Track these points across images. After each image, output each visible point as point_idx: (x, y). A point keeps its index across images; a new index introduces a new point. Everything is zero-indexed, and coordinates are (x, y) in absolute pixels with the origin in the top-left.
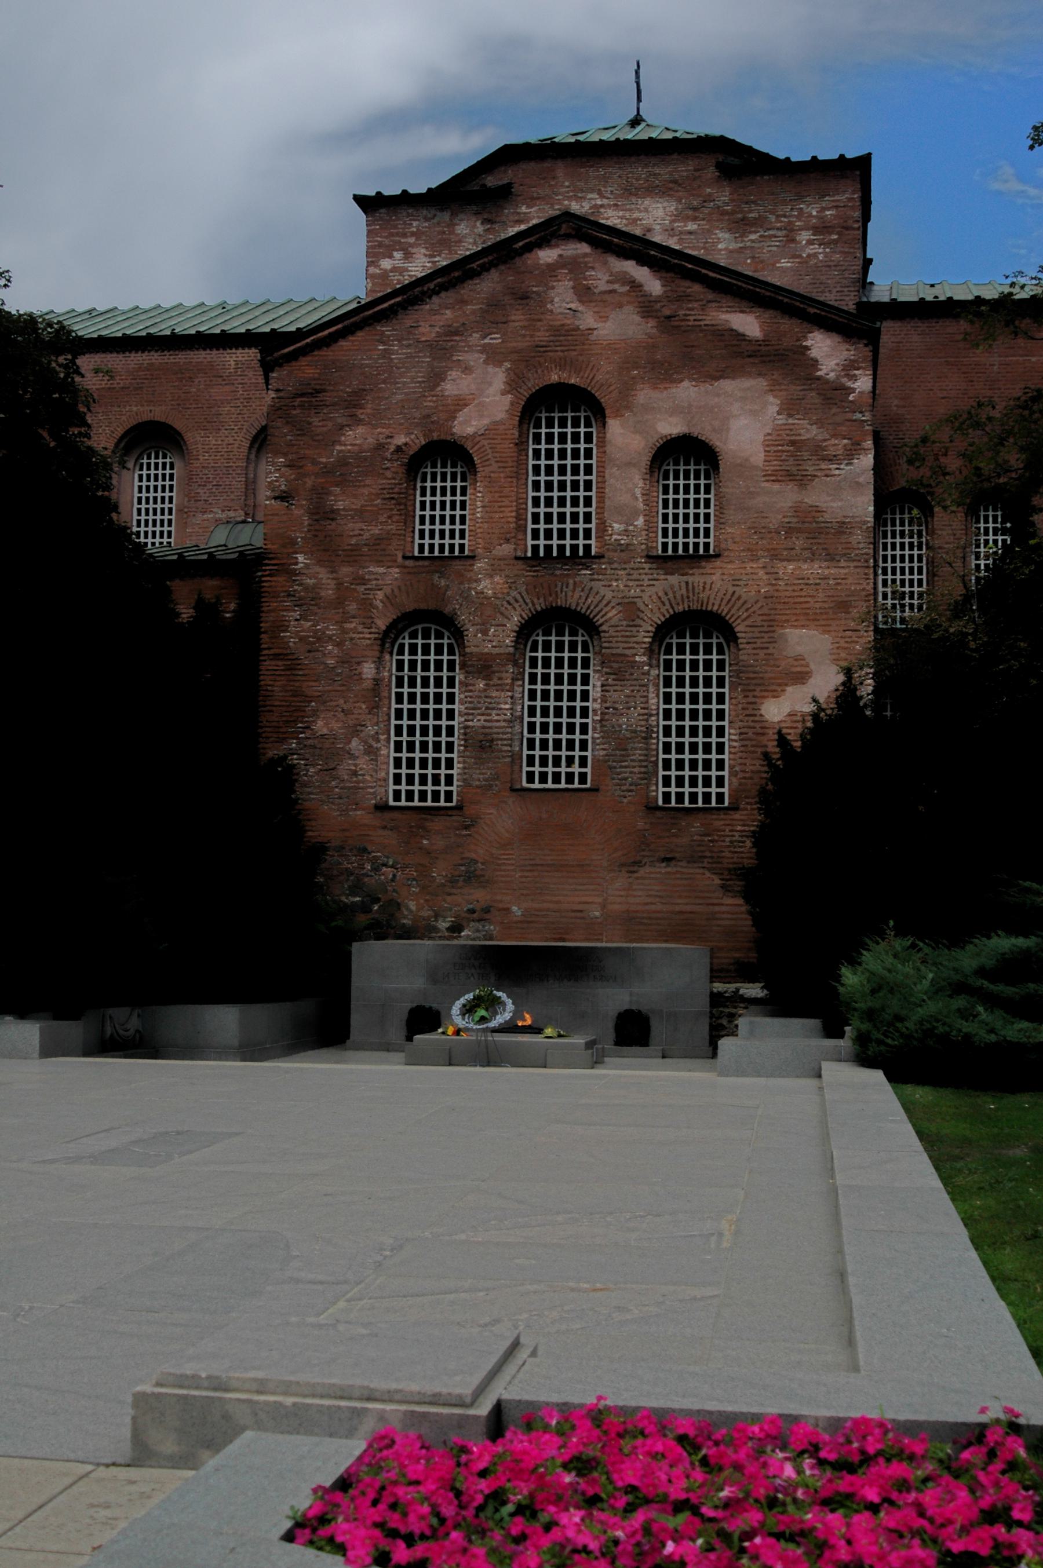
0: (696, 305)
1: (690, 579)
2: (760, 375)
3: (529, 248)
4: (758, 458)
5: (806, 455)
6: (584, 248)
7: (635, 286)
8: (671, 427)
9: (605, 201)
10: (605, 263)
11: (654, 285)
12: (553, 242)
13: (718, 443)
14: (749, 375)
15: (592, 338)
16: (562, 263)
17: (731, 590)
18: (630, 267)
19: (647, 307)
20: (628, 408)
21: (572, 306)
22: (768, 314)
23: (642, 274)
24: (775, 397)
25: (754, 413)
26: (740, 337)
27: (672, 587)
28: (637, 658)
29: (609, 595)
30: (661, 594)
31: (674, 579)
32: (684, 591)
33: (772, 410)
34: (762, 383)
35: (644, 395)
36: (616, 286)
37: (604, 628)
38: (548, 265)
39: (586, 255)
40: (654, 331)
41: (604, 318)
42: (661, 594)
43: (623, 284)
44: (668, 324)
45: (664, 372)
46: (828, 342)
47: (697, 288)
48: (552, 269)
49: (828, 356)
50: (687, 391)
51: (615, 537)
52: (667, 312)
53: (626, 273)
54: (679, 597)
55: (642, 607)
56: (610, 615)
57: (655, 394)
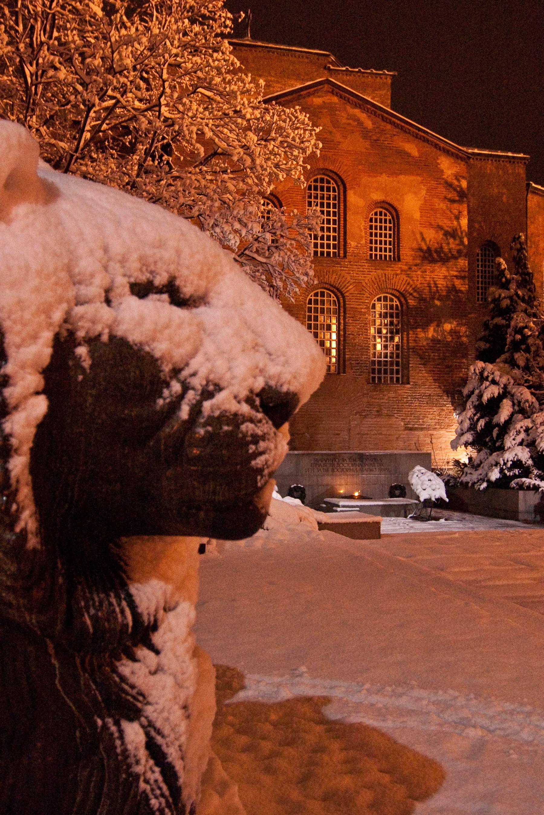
0: (388, 136)
1: (387, 272)
2: (418, 175)
3: (309, 95)
4: (417, 215)
5: (438, 216)
6: (335, 99)
7: (360, 123)
8: (377, 196)
9: (273, 79)
10: (345, 109)
11: (369, 124)
12: (320, 94)
13: (398, 206)
14: (412, 174)
15: (340, 147)
16: (324, 105)
17: (406, 278)
18: (357, 112)
19: (366, 134)
20: (358, 185)
21: (329, 129)
22: (422, 144)
23: (363, 116)
24: (424, 186)
25: (415, 193)
26: (409, 155)
27: (378, 276)
28: (363, 310)
29: (349, 278)
30: (373, 279)
31: (379, 272)
32: (384, 278)
33: (424, 192)
34: (419, 178)
35: (365, 179)
36: (351, 121)
37: (347, 294)
38: (318, 106)
39: (336, 104)
40: (369, 147)
41: (345, 137)
42: (373, 279)
43: (355, 120)
44: (375, 144)
45: (374, 169)
46: (448, 162)
47: (389, 127)
48: (320, 107)
49: (448, 169)
50: (384, 179)
51: (351, 249)
52: (375, 138)
53: (355, 115)
54: (381, 280)
55: (365, 285)
56: (350, 287)
57: (370, 179)
